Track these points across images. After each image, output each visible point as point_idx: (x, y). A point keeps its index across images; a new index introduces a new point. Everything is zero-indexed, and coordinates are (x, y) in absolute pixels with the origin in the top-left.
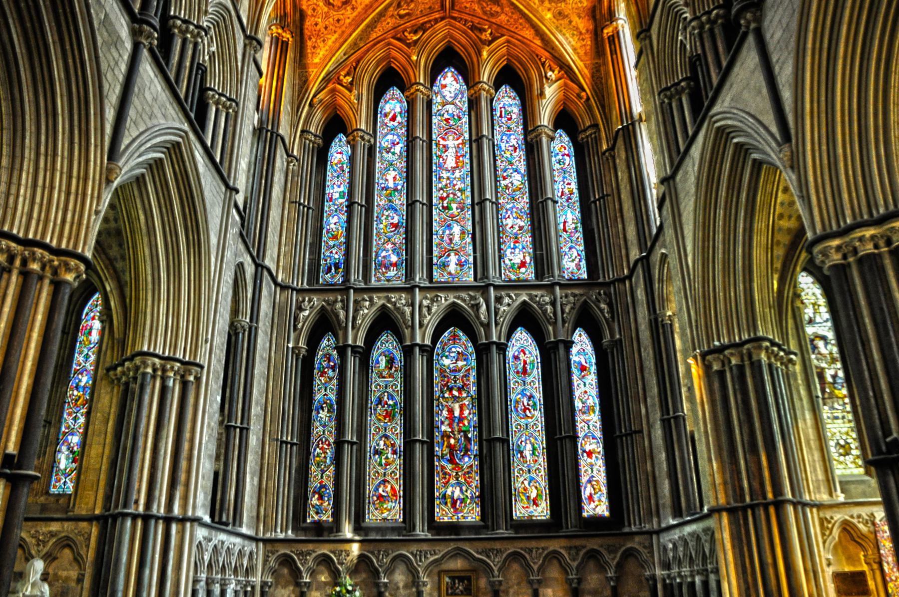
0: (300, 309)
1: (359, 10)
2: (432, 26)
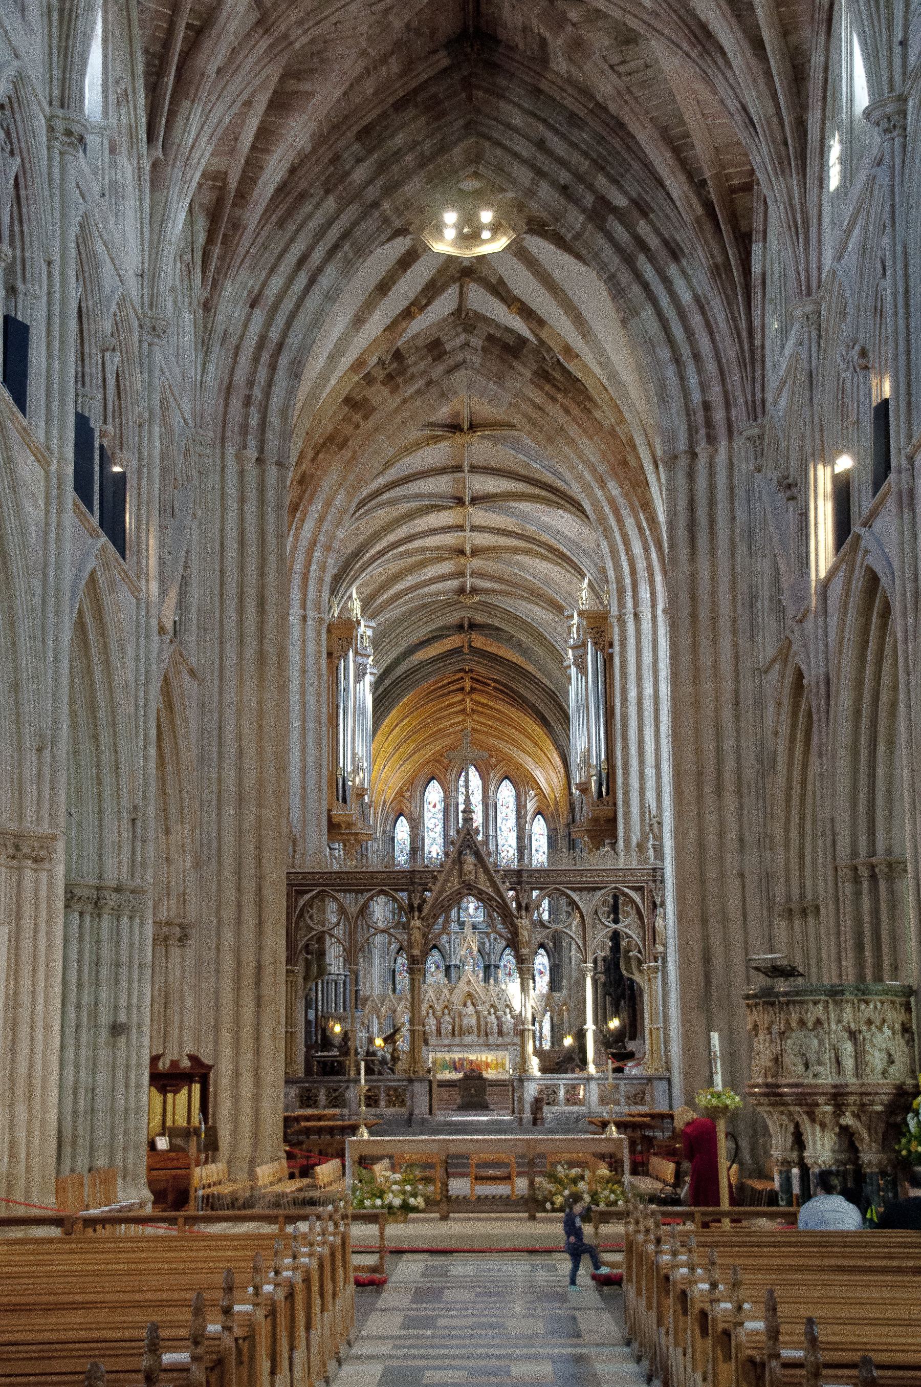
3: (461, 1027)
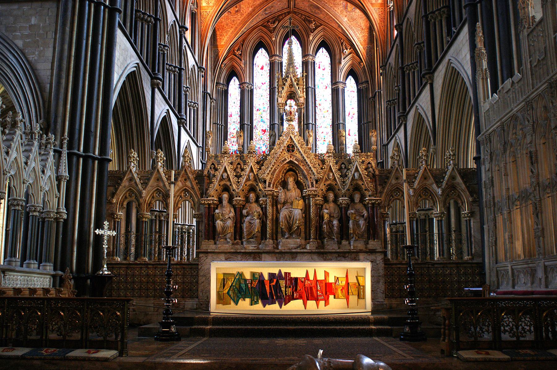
1: (244, 16)
2: (283, 18)
3: (276, 221)
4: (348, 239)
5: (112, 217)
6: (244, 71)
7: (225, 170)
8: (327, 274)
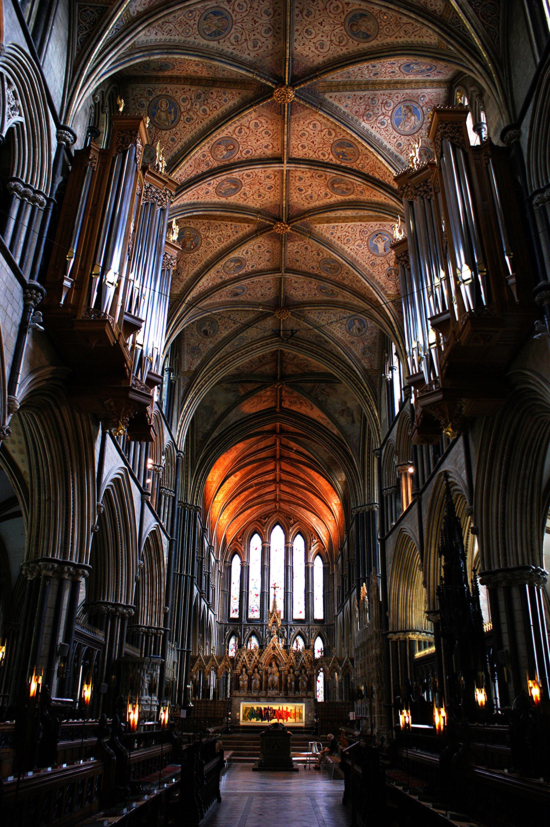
0: (226, 631)
3: (267, 682)
4: (299, 691)
5: (192, 677)
6: (243, 553)
7: (244, 658)
8: (287, 708)
